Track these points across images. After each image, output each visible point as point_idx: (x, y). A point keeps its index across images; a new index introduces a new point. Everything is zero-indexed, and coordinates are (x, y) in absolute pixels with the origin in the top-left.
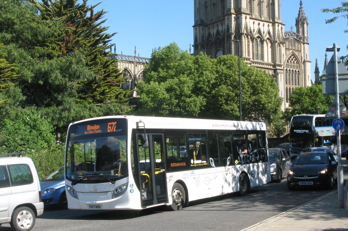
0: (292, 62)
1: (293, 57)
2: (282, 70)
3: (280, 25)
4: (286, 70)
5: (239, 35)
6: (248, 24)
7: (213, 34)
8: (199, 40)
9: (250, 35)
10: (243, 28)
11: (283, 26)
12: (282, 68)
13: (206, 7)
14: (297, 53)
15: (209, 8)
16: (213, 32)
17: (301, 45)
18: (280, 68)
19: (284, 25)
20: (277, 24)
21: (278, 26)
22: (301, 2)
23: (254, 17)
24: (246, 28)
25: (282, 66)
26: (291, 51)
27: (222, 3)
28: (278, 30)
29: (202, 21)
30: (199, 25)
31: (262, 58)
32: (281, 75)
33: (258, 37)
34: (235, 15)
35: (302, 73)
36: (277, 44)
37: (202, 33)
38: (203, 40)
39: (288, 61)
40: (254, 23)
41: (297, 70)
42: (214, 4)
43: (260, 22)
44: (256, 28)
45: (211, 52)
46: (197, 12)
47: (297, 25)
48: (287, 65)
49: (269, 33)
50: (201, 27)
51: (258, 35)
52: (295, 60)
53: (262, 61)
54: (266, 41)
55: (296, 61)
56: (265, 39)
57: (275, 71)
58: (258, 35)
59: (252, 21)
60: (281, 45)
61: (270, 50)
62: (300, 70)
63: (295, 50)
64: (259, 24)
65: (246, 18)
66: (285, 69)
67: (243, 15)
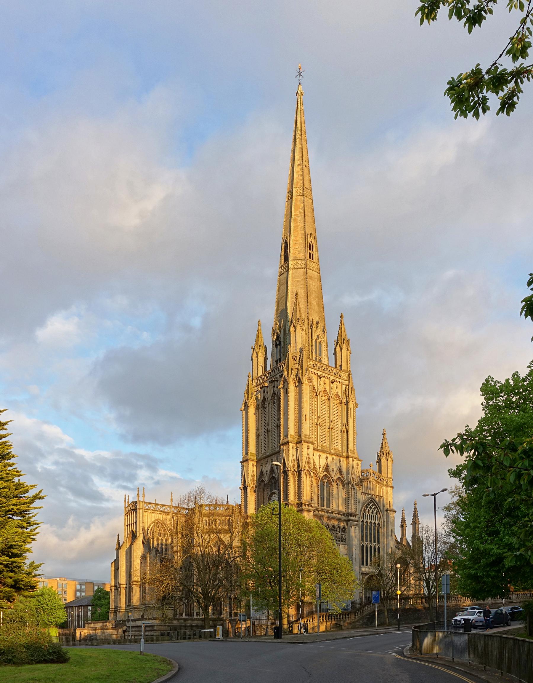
0: (371, 511)
1: (371, 504)
3: (355, 460)
10: (304, 461)
11: (359, 462)
12: (357, 519)
17: (383, 489)
18: (354, 518)
21: (353, 461)
26: (370, 496)
33: (325, 476)
35: (384, 526)
40: (320, 456)
41: (377, 523)
43: (328, 455)
44: (323, 462)
49: (340, 471)
51: (325, 473)
58: (325, 473)
59: (317, 454)
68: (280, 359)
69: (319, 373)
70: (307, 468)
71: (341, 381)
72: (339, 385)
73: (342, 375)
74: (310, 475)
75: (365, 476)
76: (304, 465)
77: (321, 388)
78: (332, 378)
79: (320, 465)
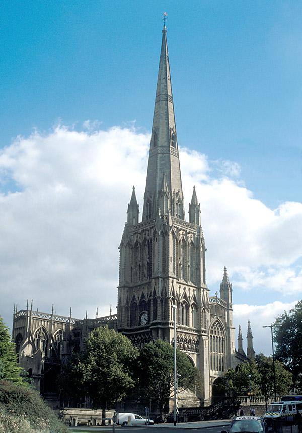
0: (217, 328)
3: (205, 290)
4: (211, 336)
5: (165, 300)
8: (124, 303)
11: (208, 291)
12: (207, 335)
18: (205, 334)
19: (209, 290)
20: (202, 289)
21: (204, 291)
22: (225, 268)
24: (173, 294)
29: (127, 282)
30: (125, 287)
31: (187, 324)
33: (184, 302)
34: (162, 279)
36: (202, 309)
38: (127, 303)
39: (212, 327)
40: (180, 287)
43: (186, 286)
44: (182, 292)
46: (122, 273)
50: (126, 289)
53: (187, 327)
54: (191, 306)
56: (191, 304)
57: (200, 336)
58: (184, 299)
64: (185, 289)
67: (170, 278)
68: (150, 216)
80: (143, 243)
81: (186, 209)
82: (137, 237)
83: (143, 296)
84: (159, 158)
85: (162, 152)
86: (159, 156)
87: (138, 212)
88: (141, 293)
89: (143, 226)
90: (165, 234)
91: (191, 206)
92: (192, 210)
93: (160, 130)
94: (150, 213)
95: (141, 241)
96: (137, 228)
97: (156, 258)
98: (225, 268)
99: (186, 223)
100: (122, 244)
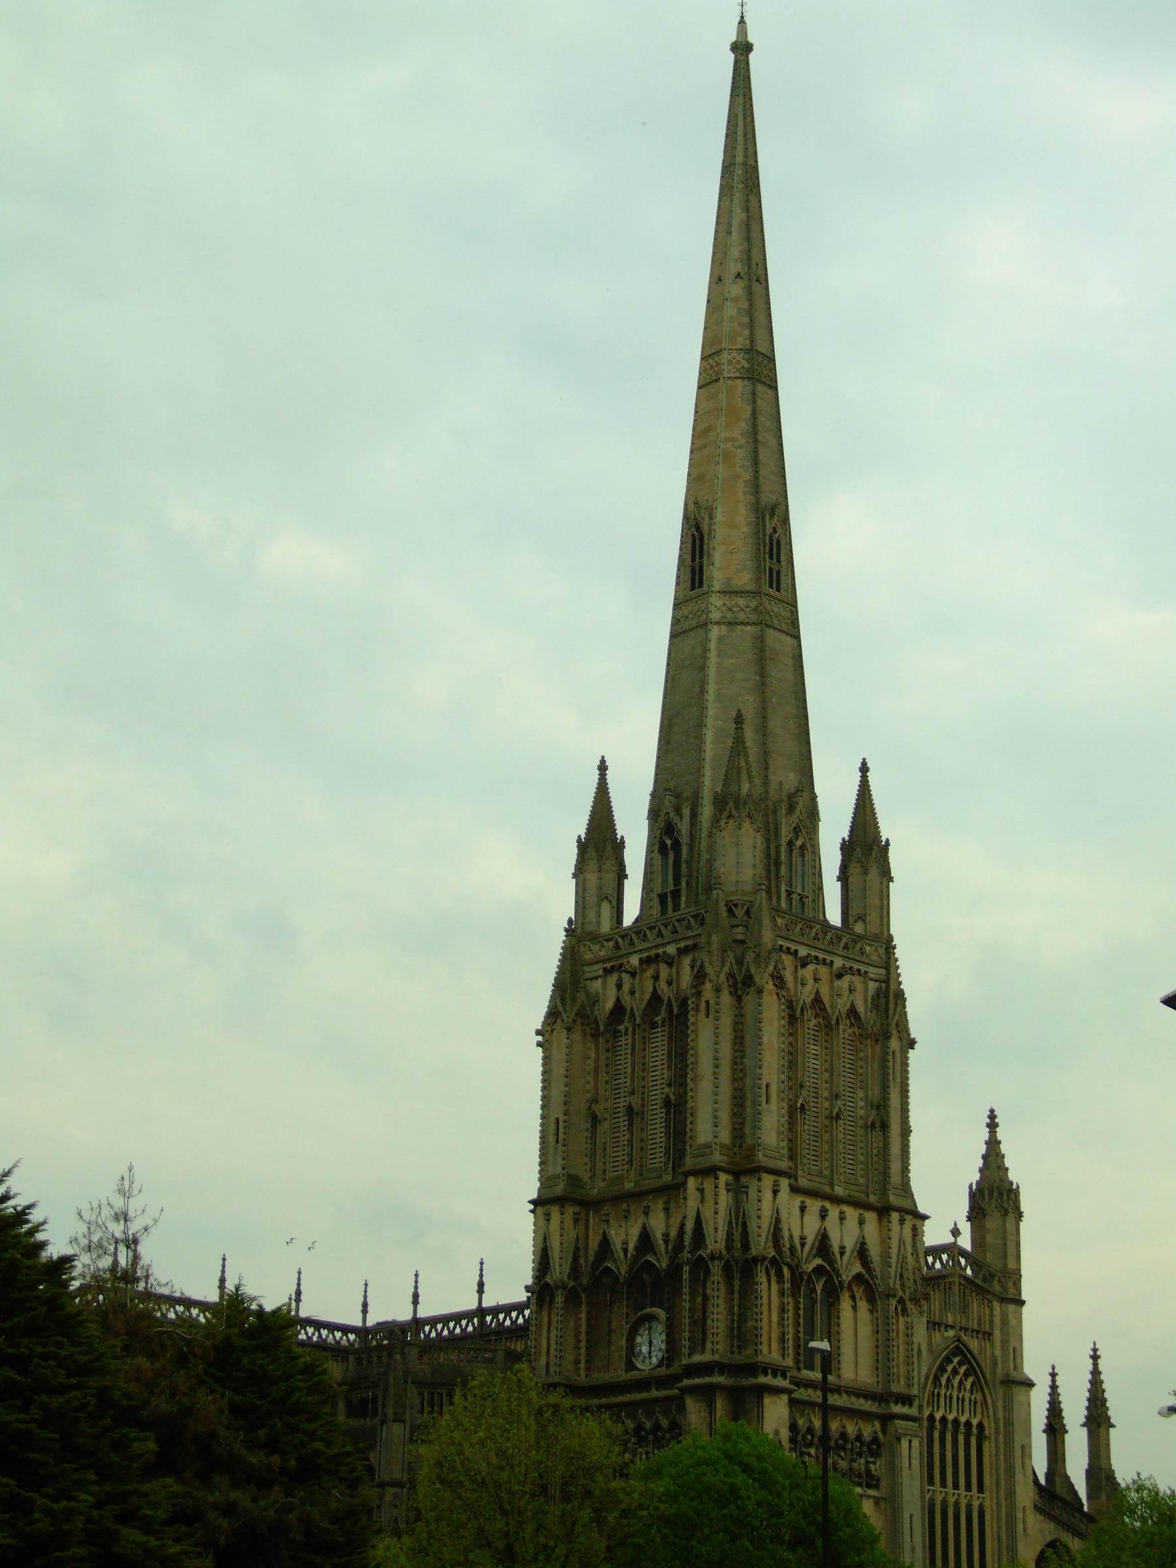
0: (956, 1382)
1: (956, 1360)
2: (913, 1419)
3: (908, 1217)
4: (931, 1418)
6: (784, 1215)
7: (625, 1243)
8: (559, 1271)
9: (781, 1260)
12: (912, 1411)
13: (595, 1120)
14: (974, 1344)
15: (606, 1125)
16: (622, 1237)
17: (992, 1309)
21: (902, 1221)
22: (992, 1116)
23: (803, 1182)
25: (916, 1403)
26: (951, 1333)
27: (668, 1113)
28: (901, 1242)
29: (574, 1181)
30: (561, 1201)
32: (910, 1442)
33: (819, 1270)
34: (730, 1178)
35: (997, 1433)
37: (573, 1236)
38: (575, 1267)
40: (803, 1209)
41: (975, 1422)
42: (630, 1110)
43: (827, 1205)
44: (812, 1225)
45: (610, 1324)
46: (552, 1139)
47: (976, 1213)
48: (934, 1398)
49: (862, 1253)
50: (570, 1210)
51: (818, 1261)
52: (966, 1375)
54: (850, 1288)
55: (970, 1380)
56: (847, 1277)
58: (818, 1261)
59: (798, 1200)
60: (909, 1305)
61: (865, 1330)
62: (989, 1423)
63: (966, 1330)
64: (823, 1214)
65: (775, 1192)
66: (927, 1413)
67: (764, 1176)
68: (676, 894)
69: (803, 951)
70: (772, 1253)
71: (863, 968)
72: (857, 981)
73: (867, 949)
74: (779, 1275)
75: (938, 1265)
76: (761, 1245)
77: (806, 995)
78: (838, 963)
79: (803, 1238)
80: (645, 1013)
81: (830, 860)
82: (619, 986)
83: (646, 1241)
84: (713, 645)
85: (729, 615)
86: (715, 632)
87: (622, 875)
88: (635, 1231)
89: (645, 938)
90: (742, 984)
91: (847, 848)
92: (855, 869)
93: (720, 516)
94: (677, 880)
95: (636, 1004)
96: (617, 946)
97: (905, 1473)
98: (992, 1116)
99: (826, 925)
100: (553, 1015)
